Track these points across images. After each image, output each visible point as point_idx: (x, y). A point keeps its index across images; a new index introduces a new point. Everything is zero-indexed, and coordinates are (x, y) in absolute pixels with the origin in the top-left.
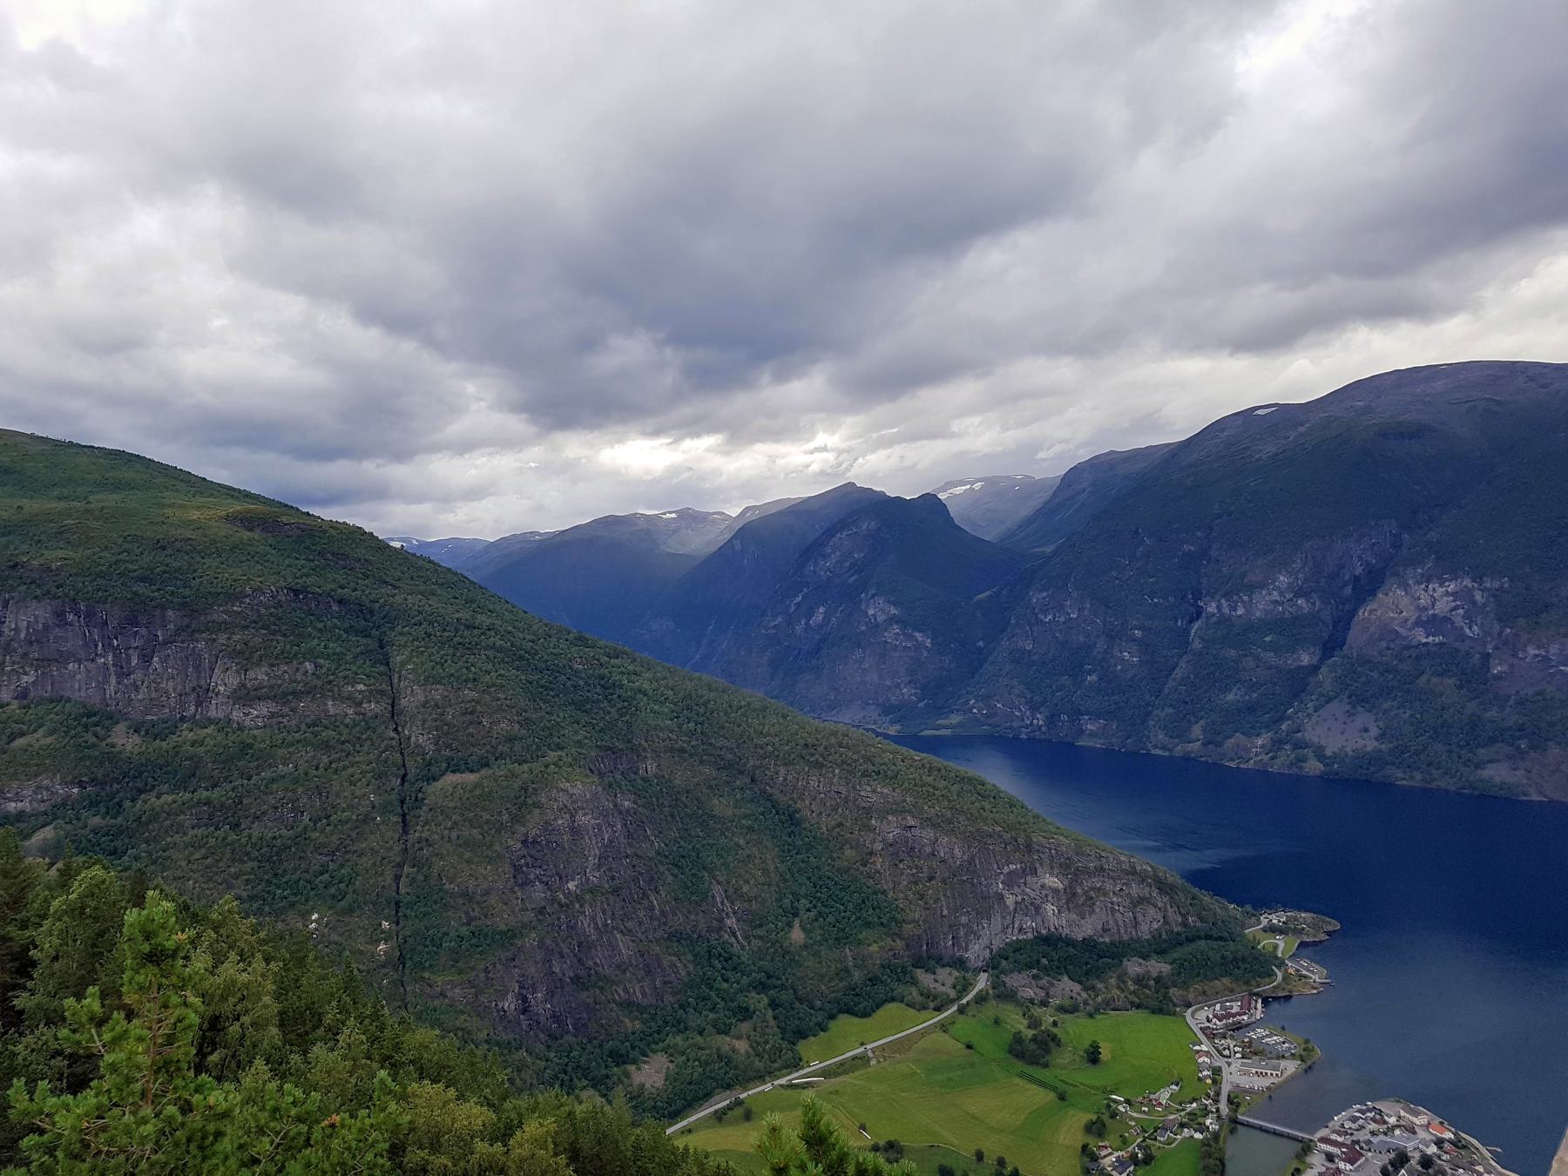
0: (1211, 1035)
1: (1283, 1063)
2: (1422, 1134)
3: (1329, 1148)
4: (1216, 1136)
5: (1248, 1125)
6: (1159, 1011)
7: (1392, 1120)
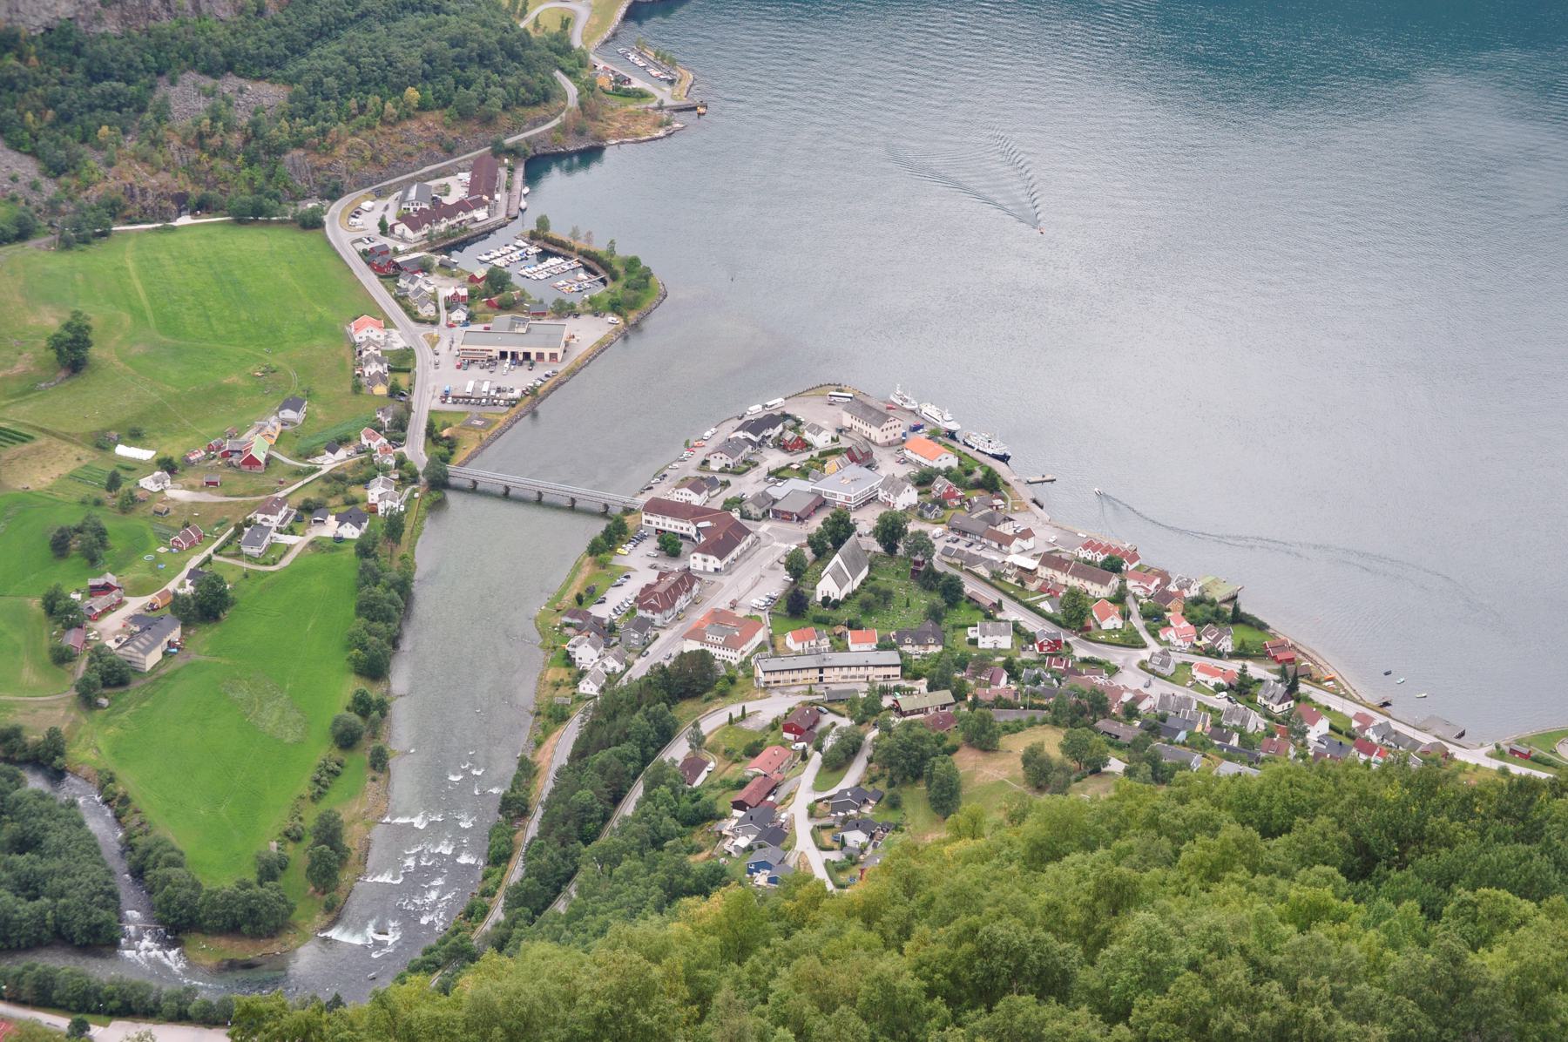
0: (387, 268)
1: (571, 325)
2: (889, 466)
3: (671, 524)
4: (394, 527)
5: (473, 490)
6: (250, 215)
7: (821, 441)
